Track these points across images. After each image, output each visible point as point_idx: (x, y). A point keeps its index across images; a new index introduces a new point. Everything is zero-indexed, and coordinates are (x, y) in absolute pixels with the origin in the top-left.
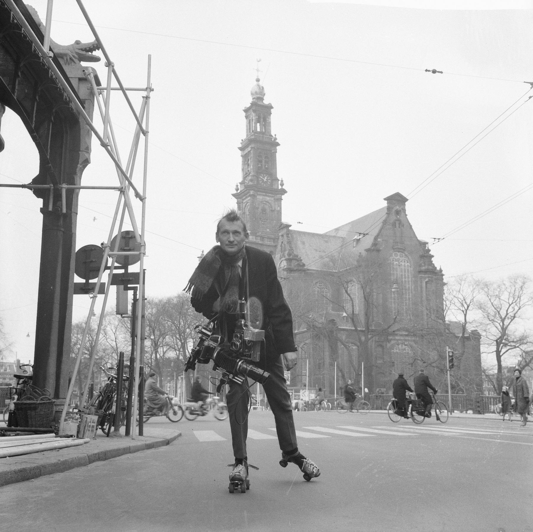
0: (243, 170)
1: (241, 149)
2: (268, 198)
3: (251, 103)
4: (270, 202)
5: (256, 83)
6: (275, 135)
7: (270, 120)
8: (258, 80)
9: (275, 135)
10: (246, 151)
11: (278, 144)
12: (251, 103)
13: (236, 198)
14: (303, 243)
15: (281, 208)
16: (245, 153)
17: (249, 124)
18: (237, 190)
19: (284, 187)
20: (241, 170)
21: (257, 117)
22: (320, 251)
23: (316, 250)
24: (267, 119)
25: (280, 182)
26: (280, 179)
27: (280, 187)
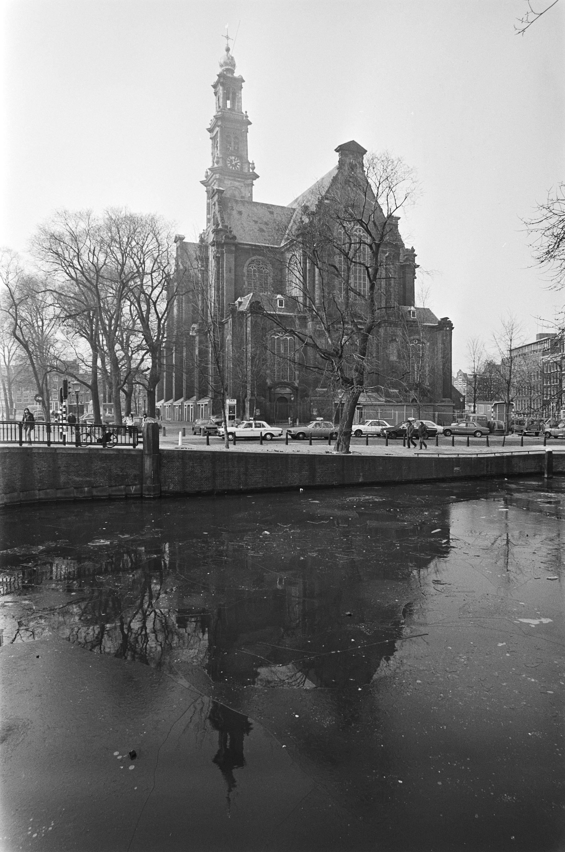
0: (212, 154)
1: (210, 130)
2: (237, 184)
3: (218, 75)
4: (240, 187)
5: (226, 53)
6: (246, 112)
7: (240, 96)
8: (228, 50)
9: (246, 112)
10: (215, 133)
11: (250, 123)
12: (218, 75)
13: (205, 186)
14: (240, 213)
15: (251, 195)
16: (214, 135)
17: (218, 102)
18: (206, 177)
19: (254, 171)
20: (210, 154)
21: (225, 91)
22: (260, 223)
23: (256, 222)
24: (237, 94)
25: (251, 165)
26: (251, 162)
27: (251, 171)
